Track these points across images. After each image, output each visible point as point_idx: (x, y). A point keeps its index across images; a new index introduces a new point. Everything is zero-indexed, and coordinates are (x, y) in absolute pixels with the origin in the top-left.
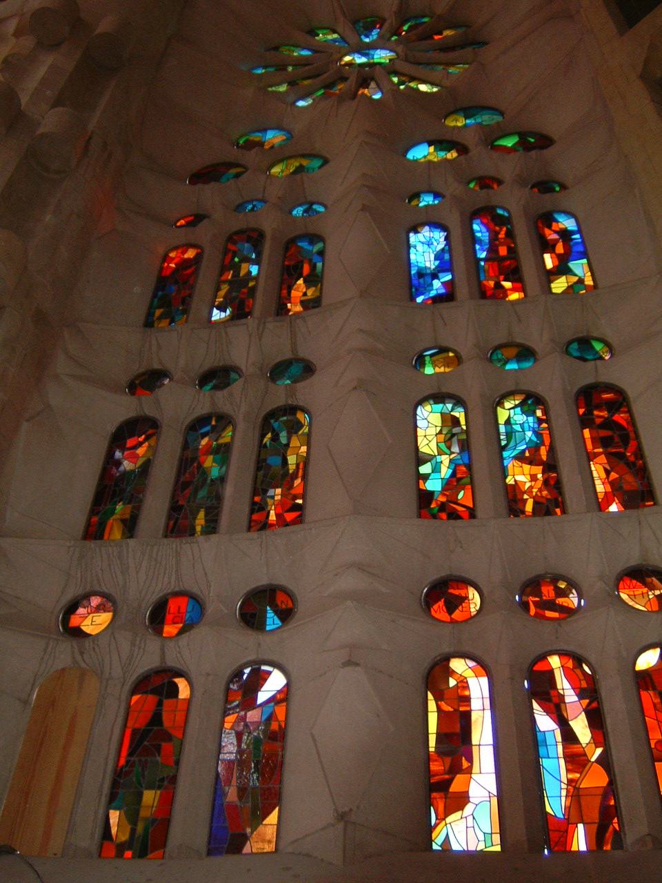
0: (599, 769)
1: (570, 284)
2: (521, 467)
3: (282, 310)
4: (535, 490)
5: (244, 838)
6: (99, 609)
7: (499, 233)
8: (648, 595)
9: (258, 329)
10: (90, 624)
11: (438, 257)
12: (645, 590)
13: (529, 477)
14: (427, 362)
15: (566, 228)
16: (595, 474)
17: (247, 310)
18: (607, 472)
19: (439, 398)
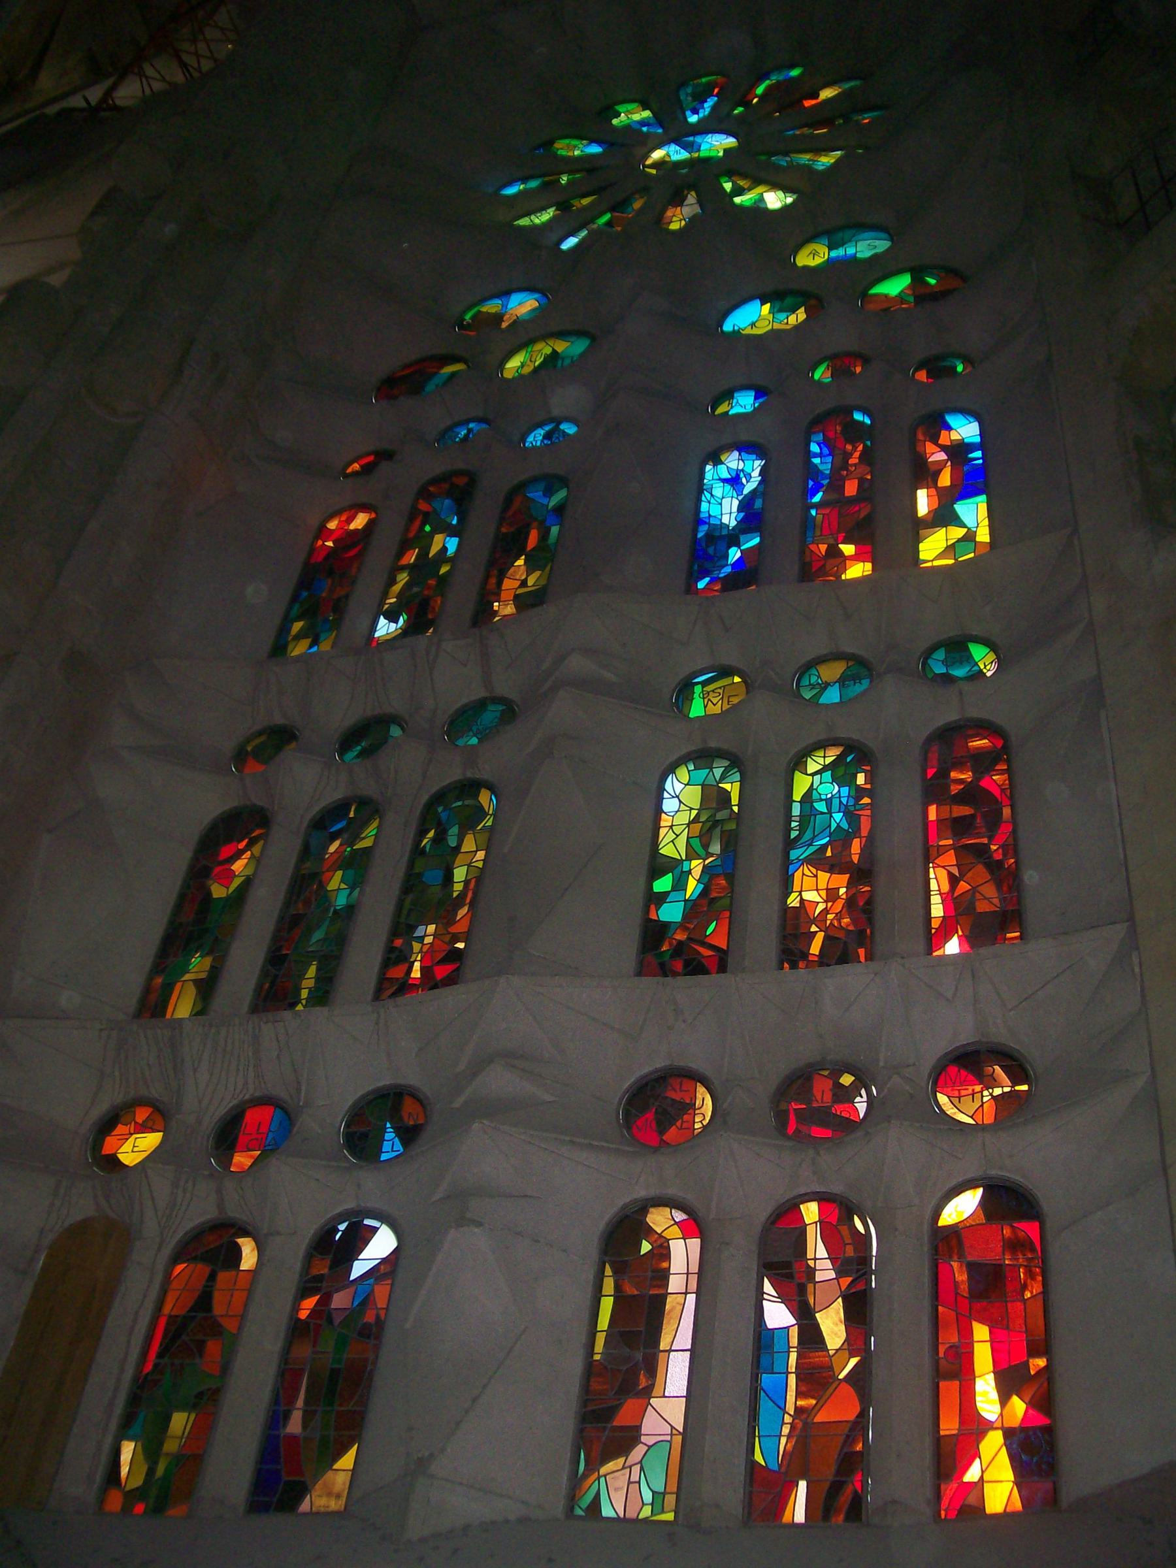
0: (848, 1390)
1: (950, 543)
2: (816, 876)
3: (483, 614)
4: (830, 917)
5: (300, 1490)
6: (143, 1128)
7: (850, 455)
8: (982, 1096)
9: (428, 653)
10: (130, 1151)
11: (746, 505)
12: (978, 1088)
13: (823, 893)
14: (696, 696)
15: (963, 439)
16: (934, 885)
17: (430, 616)
18: (953, 880)
19: (702, 757)
